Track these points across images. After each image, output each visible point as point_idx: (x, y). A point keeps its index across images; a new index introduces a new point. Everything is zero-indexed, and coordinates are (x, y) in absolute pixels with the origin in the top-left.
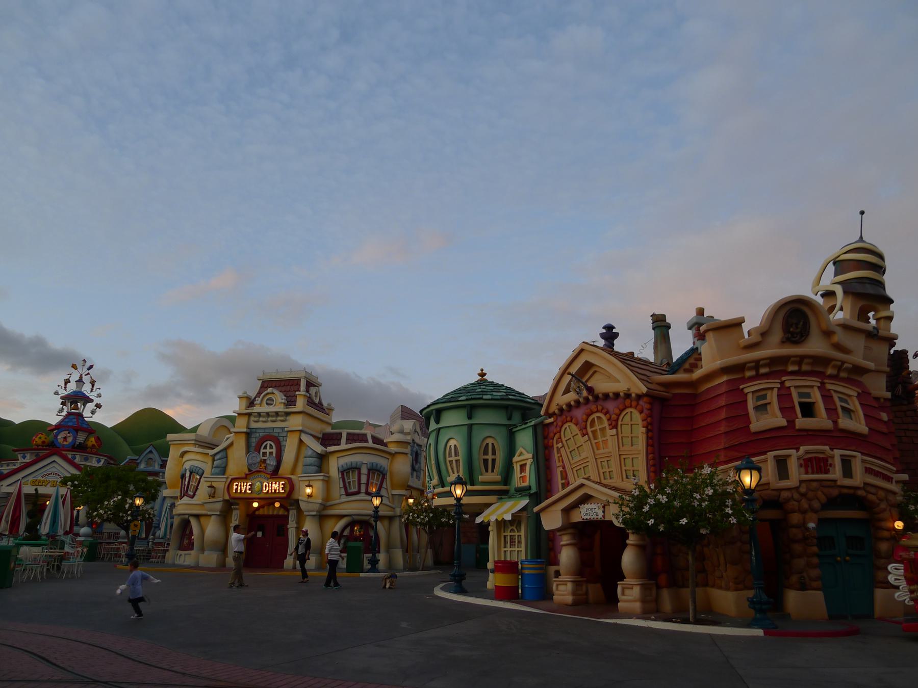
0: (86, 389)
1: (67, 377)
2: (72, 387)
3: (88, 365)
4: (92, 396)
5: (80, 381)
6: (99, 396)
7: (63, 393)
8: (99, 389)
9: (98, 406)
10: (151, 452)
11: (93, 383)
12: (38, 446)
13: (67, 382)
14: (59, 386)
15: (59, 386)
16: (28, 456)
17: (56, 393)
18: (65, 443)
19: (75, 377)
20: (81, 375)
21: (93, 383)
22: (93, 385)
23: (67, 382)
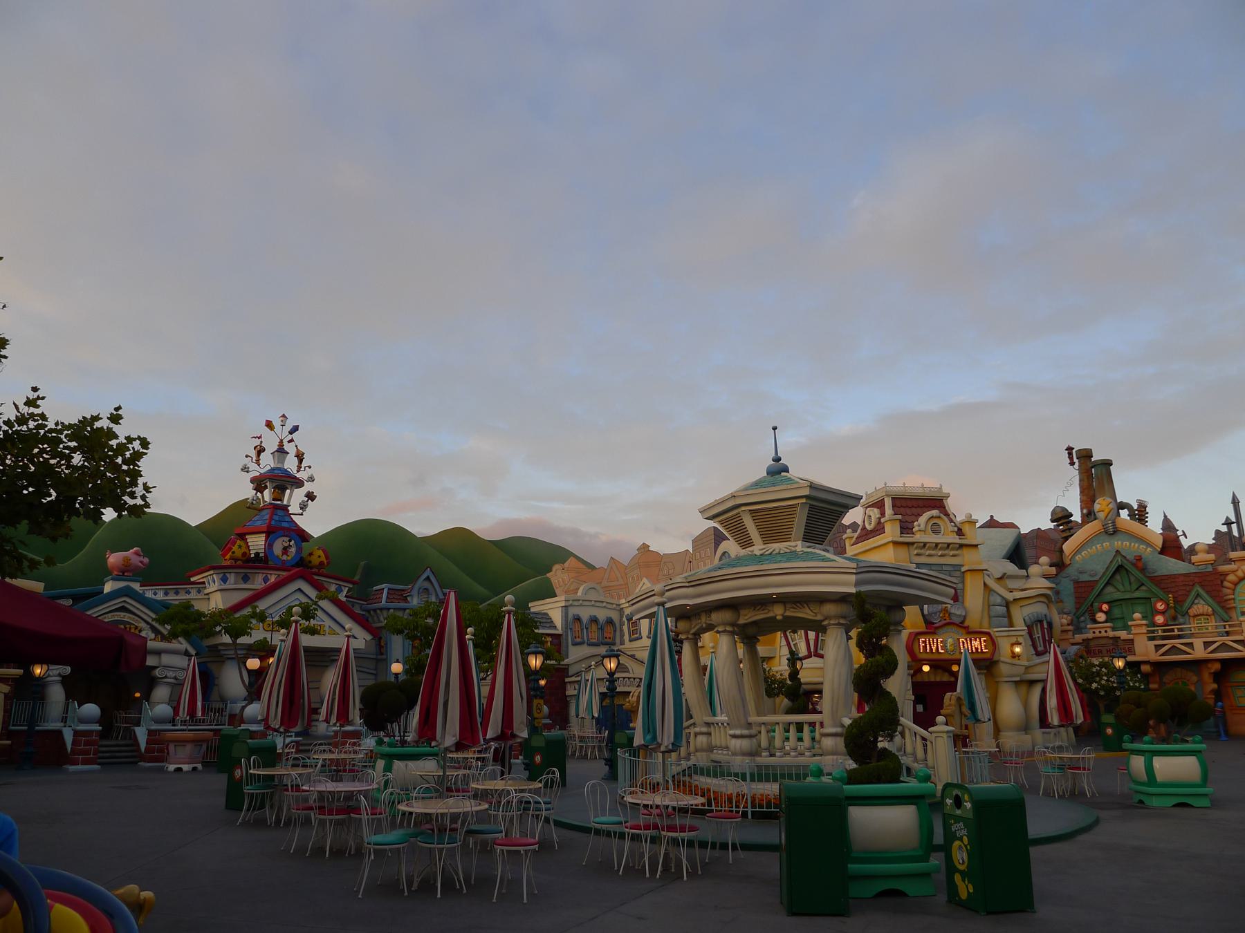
0: (290, 464)
1: (257, 442)
2: (268, 461)
3: (289, 427)
4: (302, 475)
5: (281, 451)
6: (311, 479)
7: (256, 471)
8: (310, 467)
9: (311, 496)
10: (428, 579)
11: (300, 457)
12: (236, 560)
13: (260, 450)
14: (247, 456)
15: (247, 456)
16: (232, 578)
17: (245, 469)
18: (285, 557)
19: (271, 445)
20: (281, 441)
21: (300, 457)
22: (301, 461)
23: (260, 450)
